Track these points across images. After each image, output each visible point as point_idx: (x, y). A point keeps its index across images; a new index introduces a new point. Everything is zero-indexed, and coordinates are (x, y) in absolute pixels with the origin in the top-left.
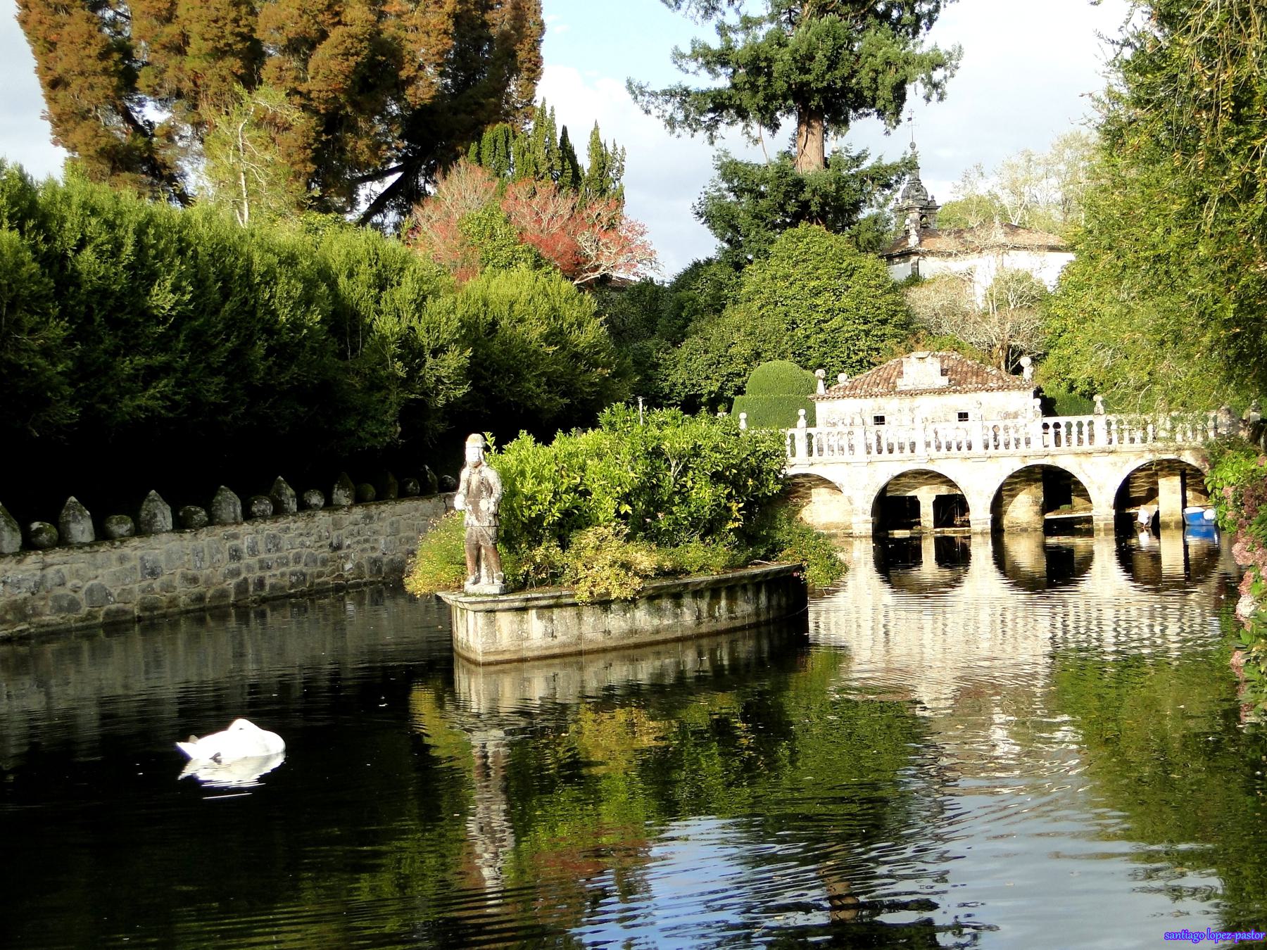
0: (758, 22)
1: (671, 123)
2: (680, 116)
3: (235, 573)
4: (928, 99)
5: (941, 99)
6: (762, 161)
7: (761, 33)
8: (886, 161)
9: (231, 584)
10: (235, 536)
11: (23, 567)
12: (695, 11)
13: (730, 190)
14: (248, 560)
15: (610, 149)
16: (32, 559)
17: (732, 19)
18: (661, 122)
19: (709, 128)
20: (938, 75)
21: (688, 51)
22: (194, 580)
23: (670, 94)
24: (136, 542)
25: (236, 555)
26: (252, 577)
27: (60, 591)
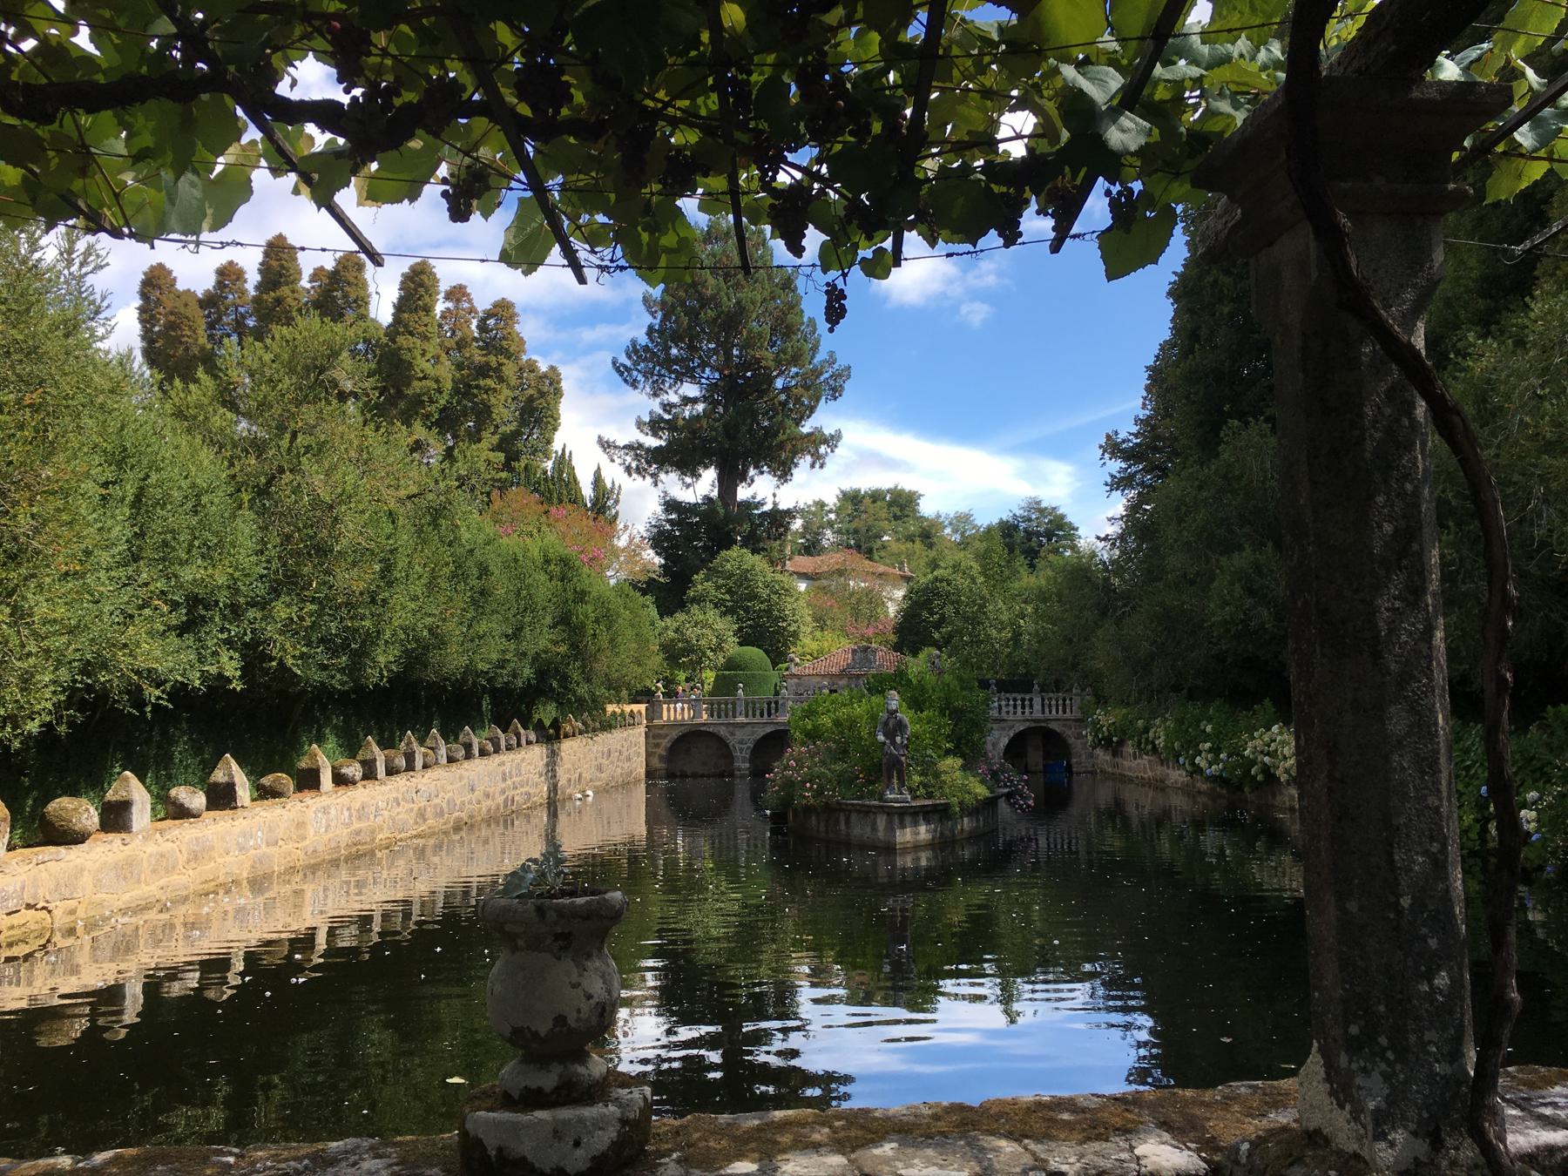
0: (694, 401)
1: (628, 470)
2: (634, 465)
3: (503, 792)
4: (813, 466)
5: (822, 467)
6: (693, 501)
7: (700, 407)
8: (783, 506)
9: (500, 800)
10: (503, 764)
11: (425, 780)
12: (648, 389)
13: (668, 521)
14: (509, 782)
15: (609, 485)
16: (429, 773)
17: (674, 399)
18: (622, 469)
19: (652, 475)
20: (823, 449)
21: (647, 419)
22: (488, 796)
23: (629, 447)
24: (466, 764)
25: (504, 780)
26: (510, 793)
27: (436, 801)
